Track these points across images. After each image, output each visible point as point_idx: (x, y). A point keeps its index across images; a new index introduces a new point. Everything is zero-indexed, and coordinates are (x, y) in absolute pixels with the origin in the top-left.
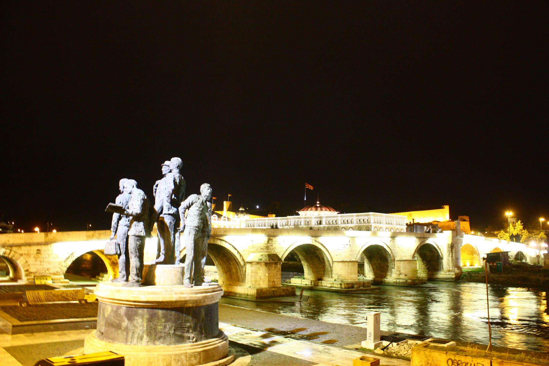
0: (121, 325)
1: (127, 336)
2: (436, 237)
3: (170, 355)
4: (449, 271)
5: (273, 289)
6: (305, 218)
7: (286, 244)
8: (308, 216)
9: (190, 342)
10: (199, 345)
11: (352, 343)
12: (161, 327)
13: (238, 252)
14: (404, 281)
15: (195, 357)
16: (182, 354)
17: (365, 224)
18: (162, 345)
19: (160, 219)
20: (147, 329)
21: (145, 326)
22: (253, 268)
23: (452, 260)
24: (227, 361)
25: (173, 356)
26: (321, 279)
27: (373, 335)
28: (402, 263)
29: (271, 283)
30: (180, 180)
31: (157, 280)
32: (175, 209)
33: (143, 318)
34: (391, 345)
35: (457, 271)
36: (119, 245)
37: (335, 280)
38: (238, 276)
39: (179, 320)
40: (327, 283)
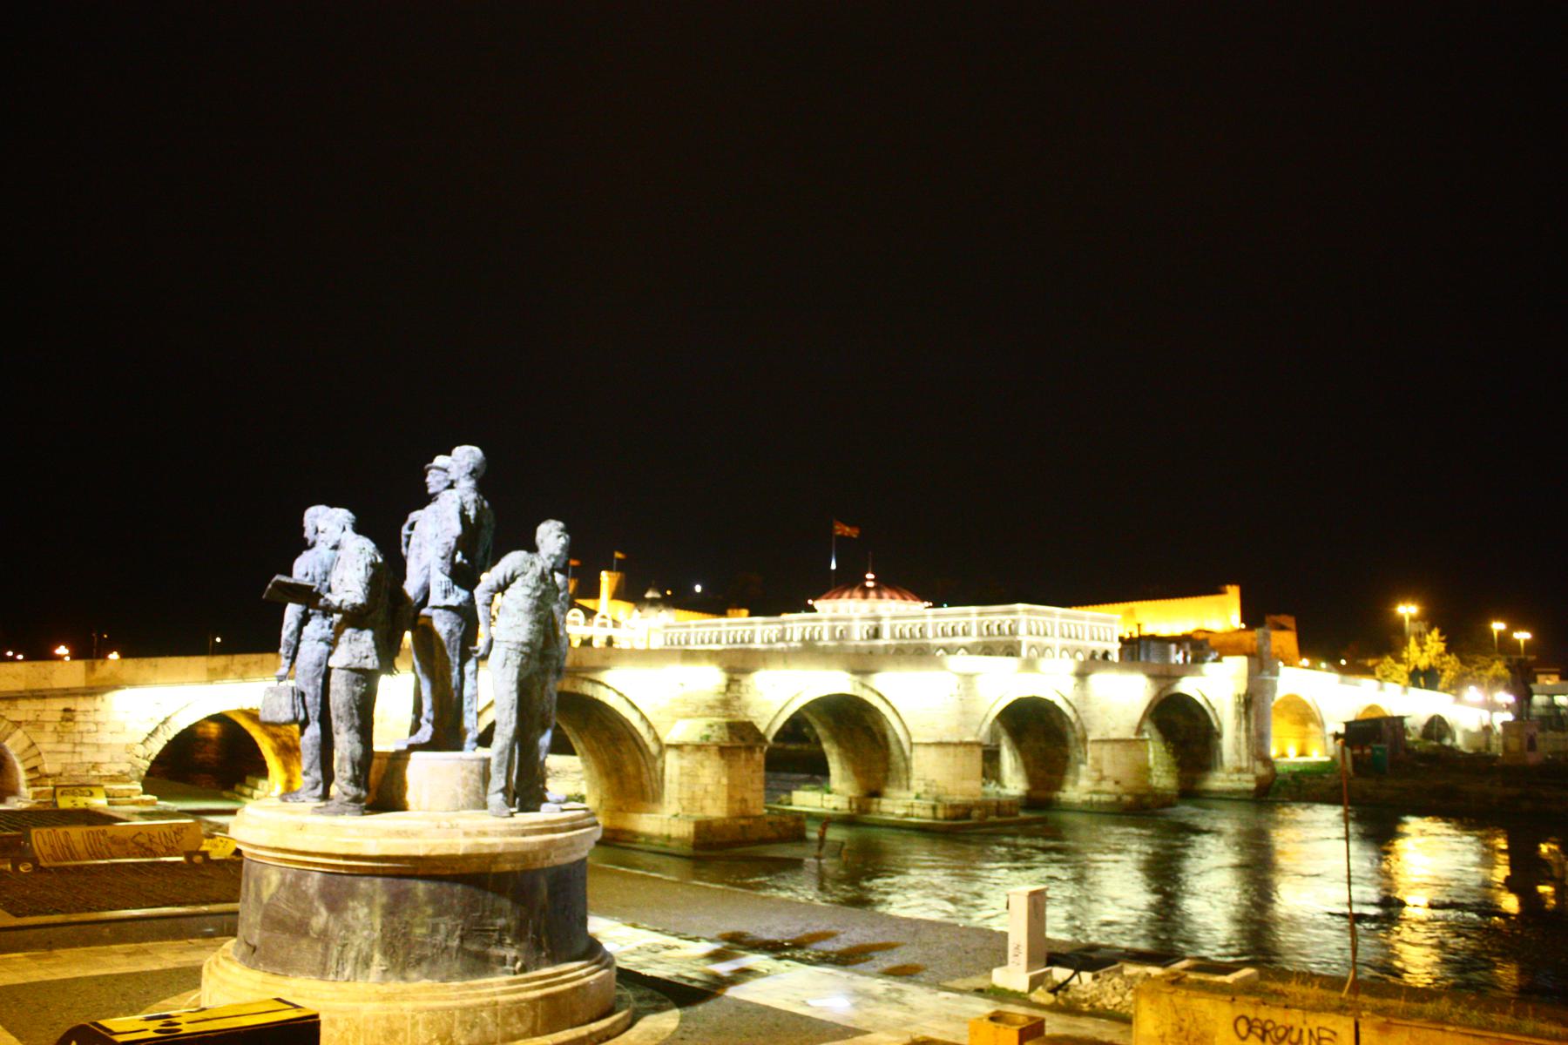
0: (307, 924)
1: (326, 954)
2: (1201, 674)
3: (447, 1009)
4: (1240, 770)
5: (743, 822)
6: (833, 620)
7: (775, 697)
8: (841, 613)
9: (507, 972)
10: (534, 979)
11: (966, 975)
12: (424, 931)
13: (643, 717)
14: (1113, 798)
16: (482, 1006)
17: (1001, 639)
18: (426, 982)
19: (421, 622)
20: (383, 937)
21: (378, 926)
22: (685, 763)
23: (1248, 738)
24: (613, 1025)
25: (457, 1013)
28: (1107, 747)
29: (737, 806)
30: (479, 511)
31: (410, 797)
33: (370, 902)
34: (1075, 980)
35: (1261, 770)
36: (303, 695)
37: (918, 797)
38: (642, 785)
39: (473, 909)
40: (896, 804)
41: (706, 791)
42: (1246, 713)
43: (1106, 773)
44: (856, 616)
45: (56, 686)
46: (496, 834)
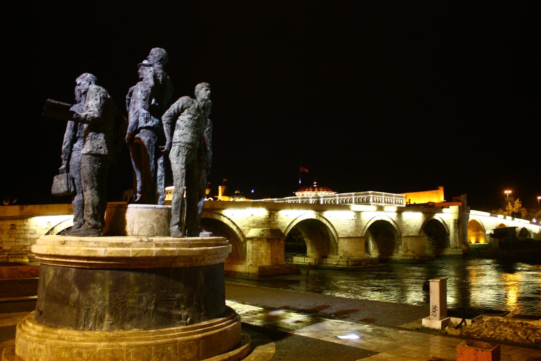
0: (68, 298)
1: (78, 315)
2: (442, 213)
3: (147, 346)
4: (456, 248)
5: (277, 267)
6: (302, 198)
7: (289, 217)
8: (305, 196)
9: (182, 324)
11: (408, 322)
12: (133, 300)
13: (238, 228)
14: (412, 258)
15: (191, 349)
16: (167, 343)
18: (135, 330)
19: (136, 141)
20: (110, 304)
21: (107, 298)
22: (254, 245)
23: (459, 236)
25: (153, 348)
26: (326, 257)
27: (438, 309)
28: (409, 239)
29: (274, 261)
30: (164, 79)
31: (128, 229)
32: (156, 121)
33: (103, 285)
34: (463, 324)
35: (464, 247)
36: (73, 179)
37: (341, 258)
40: (333, 261)
41: (262, 255)
42: (458, 226)
43: (409, 248)
44: (311, 197)
45: (8, 215)
46: (174, 245)
